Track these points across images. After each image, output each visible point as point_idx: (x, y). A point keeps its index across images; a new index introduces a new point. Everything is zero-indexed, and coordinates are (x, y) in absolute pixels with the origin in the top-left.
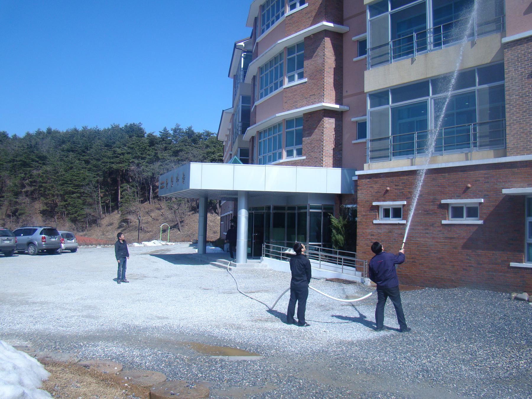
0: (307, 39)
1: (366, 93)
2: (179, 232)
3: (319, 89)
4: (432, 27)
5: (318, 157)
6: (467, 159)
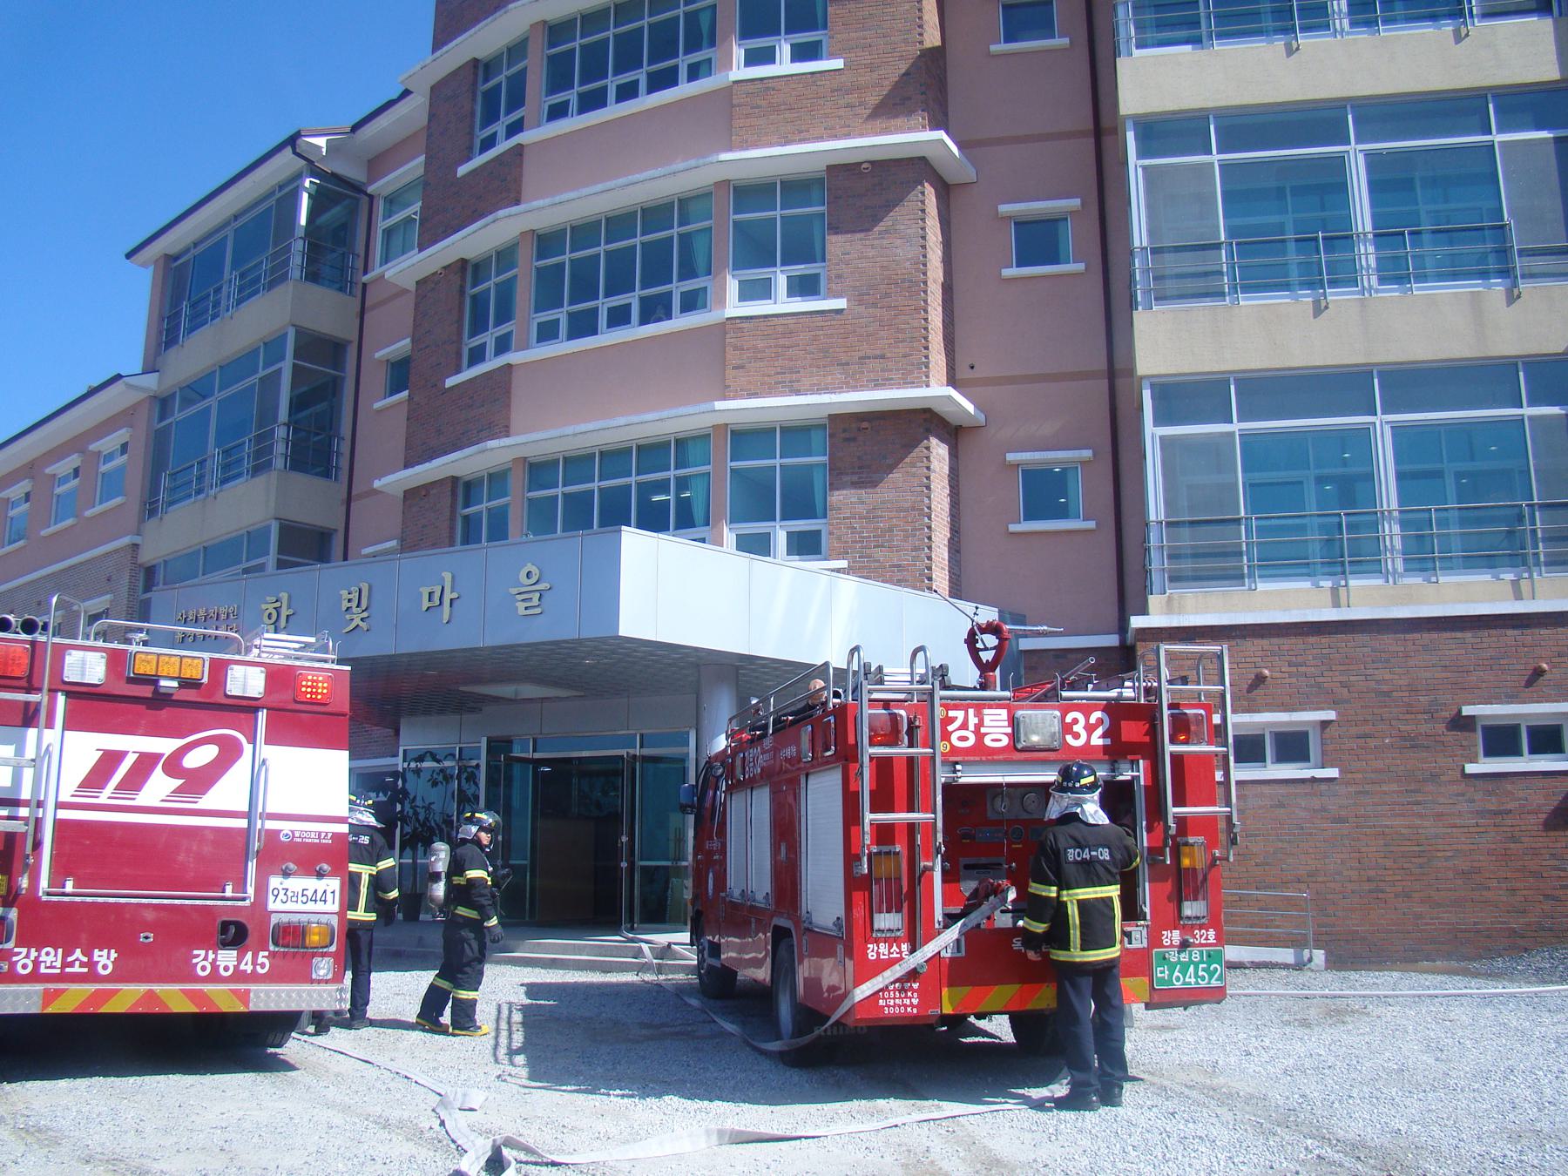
1: (1142, 378)
6: (1518, 596)
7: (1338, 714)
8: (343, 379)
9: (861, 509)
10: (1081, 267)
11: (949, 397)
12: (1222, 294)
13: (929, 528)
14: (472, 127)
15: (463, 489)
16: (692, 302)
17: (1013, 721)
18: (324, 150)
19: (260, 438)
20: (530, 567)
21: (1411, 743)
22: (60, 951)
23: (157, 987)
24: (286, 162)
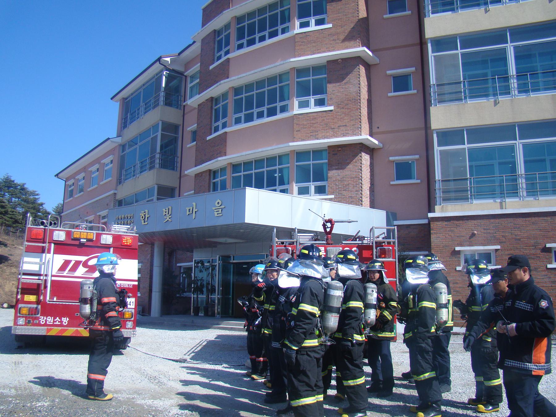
1: (433, 130)
3: (353, 120)
5: (355, 196)
7: (501, 247)
8: (178, 137)
9: (339, 178)
10: (415, 91)
11: (367, 139)
12: (461, 100)
13: (361, 184)
14: (214, 52)
15: (213, 173)
16: (284, 109)
17: (326, 251)
18: (169, 62)
19: (151, 158)
20: (219, 201)
22: (53, 318)
23: (79, 329)
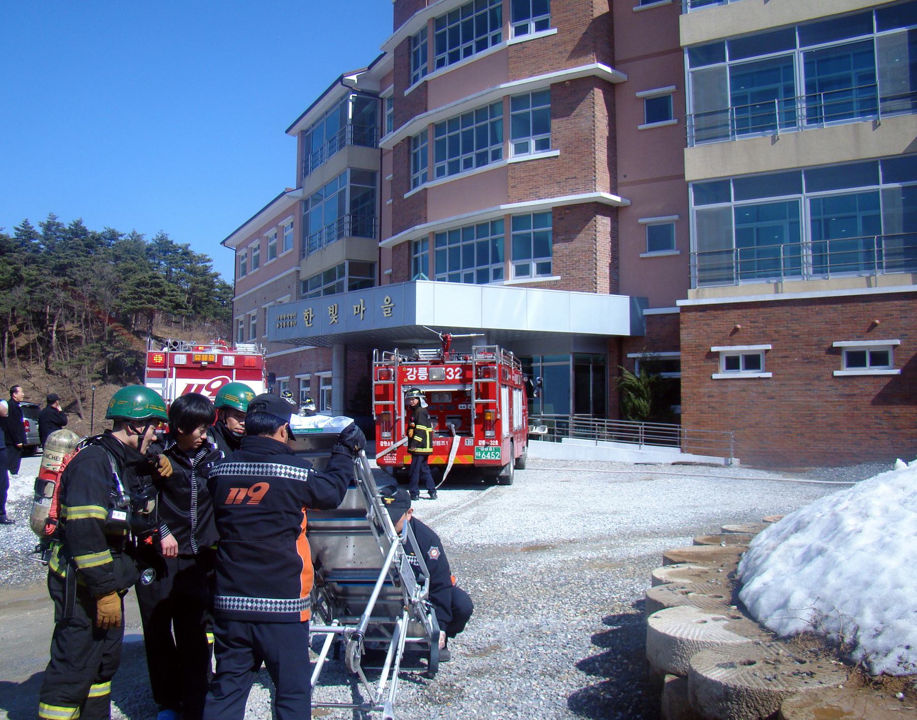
0: (558, 86)
2: (80, 421)
4: (803, 93)
6: (869, 286)
9: (566, 251)
12: (728, 136)
17: (428, 372)
20: (388, 297)
21: (807, 360)
24: (339, 90)
